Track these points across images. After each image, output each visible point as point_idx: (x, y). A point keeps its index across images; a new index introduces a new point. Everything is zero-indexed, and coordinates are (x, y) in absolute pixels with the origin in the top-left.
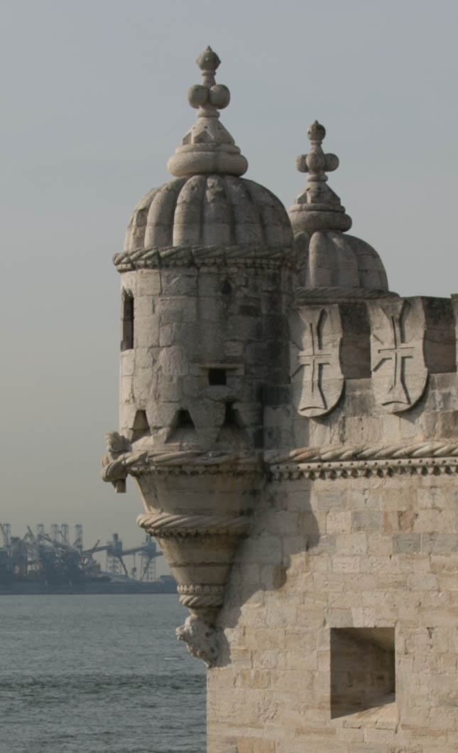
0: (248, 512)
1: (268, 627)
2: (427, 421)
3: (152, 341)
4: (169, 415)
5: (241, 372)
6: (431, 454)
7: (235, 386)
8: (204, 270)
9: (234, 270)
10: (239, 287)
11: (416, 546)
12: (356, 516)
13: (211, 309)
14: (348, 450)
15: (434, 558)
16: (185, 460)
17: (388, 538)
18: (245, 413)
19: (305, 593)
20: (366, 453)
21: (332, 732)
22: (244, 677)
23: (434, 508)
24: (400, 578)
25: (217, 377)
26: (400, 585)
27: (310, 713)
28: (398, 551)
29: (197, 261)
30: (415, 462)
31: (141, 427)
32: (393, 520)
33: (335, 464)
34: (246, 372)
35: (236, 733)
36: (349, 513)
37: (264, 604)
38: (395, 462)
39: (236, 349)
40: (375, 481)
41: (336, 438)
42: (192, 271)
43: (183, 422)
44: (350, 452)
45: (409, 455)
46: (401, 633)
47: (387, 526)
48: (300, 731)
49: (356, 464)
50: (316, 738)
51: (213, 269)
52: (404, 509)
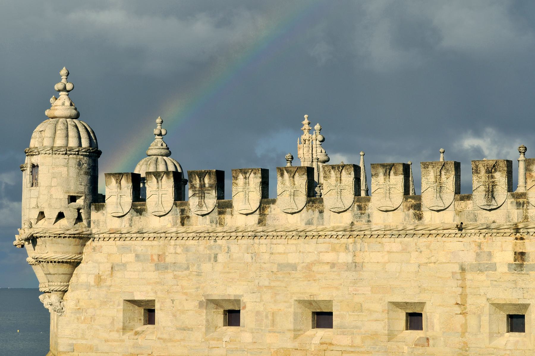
0: (81, 253)
1: (91, 299)
2: (173, 219)
5: (83, 198)
7: (80, 202)
8: (71, 156)
10: (83, 164)
11: (166, 268)
12: (137, 256)
14: (134, 230)
15: (175, 273)
17: (152, 264)
19: (110, 286)
20: (144, 231)
21: (123, 341)
22: (78, 319)
23: (176, 253)
24: (158, 280)
25: (73, 199)
27: (112, 333)
28: (158, 270)
29: (68, 152)
30: (167, 235)
32: (155, 258)
33: (127, 235)
34: (86, 198)
35: (74, 342)
36: (134, 254)
37: (89, 290)
38: (159, 235)
41: (127, 225)
43: (61, 216)
44: (137, 231)
46: (159, 301)
47: (152, 260)
48: (106, 341)
49: (138, 235)
50: (115, 343)
52: (161, 253)
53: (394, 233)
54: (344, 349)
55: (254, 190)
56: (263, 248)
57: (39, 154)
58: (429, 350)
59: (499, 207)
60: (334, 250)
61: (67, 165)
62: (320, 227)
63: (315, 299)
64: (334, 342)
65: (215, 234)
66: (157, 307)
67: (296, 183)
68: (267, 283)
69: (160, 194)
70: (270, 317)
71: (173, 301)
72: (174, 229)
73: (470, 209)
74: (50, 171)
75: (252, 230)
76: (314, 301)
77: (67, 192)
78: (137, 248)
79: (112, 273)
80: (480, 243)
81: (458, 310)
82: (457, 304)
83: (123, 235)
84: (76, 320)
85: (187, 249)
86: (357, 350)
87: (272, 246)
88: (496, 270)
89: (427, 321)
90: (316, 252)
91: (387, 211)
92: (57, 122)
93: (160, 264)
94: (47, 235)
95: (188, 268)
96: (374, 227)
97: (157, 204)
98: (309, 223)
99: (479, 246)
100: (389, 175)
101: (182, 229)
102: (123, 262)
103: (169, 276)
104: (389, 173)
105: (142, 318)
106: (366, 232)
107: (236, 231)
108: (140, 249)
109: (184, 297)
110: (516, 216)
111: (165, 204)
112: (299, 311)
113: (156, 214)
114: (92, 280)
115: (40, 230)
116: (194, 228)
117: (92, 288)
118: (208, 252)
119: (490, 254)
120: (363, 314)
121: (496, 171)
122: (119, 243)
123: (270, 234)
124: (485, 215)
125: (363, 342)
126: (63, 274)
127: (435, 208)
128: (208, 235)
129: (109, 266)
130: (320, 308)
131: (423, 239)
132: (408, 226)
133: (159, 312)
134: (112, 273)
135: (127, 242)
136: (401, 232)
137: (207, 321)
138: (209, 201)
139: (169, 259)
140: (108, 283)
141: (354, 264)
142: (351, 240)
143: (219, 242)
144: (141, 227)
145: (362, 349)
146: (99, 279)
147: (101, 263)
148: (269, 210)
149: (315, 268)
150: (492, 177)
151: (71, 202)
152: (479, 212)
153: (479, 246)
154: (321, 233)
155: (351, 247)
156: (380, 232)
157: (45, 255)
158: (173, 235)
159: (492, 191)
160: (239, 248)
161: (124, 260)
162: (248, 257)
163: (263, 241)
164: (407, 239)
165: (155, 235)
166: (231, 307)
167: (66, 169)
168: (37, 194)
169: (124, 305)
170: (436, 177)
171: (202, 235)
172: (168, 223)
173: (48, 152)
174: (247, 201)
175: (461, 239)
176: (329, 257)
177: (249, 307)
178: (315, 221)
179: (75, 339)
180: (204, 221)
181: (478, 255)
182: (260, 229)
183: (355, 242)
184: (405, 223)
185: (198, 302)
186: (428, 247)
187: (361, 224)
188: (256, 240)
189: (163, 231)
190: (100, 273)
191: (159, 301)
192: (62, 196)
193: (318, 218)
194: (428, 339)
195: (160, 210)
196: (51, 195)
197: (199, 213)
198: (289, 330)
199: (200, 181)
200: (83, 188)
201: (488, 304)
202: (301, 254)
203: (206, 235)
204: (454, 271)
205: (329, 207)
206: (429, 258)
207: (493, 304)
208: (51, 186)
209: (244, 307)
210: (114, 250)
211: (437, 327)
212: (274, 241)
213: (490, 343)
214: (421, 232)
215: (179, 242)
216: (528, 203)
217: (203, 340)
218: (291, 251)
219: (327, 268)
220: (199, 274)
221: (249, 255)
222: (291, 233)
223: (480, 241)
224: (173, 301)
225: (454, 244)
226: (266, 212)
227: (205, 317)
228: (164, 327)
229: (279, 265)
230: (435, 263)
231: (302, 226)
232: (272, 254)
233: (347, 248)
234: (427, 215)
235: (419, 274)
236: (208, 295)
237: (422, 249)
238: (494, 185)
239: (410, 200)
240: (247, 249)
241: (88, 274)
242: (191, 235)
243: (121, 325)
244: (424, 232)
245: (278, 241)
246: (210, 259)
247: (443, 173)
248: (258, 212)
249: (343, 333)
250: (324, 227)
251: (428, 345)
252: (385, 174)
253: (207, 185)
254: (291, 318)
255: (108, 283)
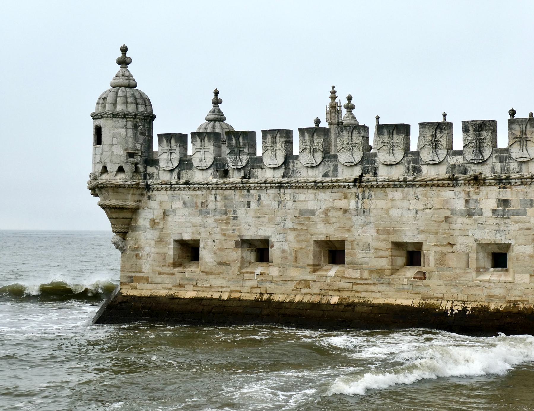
0: (140, 201)
3: (110, 142)
4: (116, 168)
5: (140, 154)
6: (217, 184)
7: (138, 159)
8: (128, 119)
9: (138, 120)
10: (139, 126)
11: (209, 213)
12: (184, 203)
13: (130, 133)
14: (182, 181)
15: (216, 217)
16: (122, 183)
18: (141, 167)
19: (163, 228)
21: (173, 274)
24: (202, 223)
25: (131, 155)
26: (201, 226)
27: (164, 268)
28: (201, 215)
31: (105, 170)
32: (199, 205)
35: (133, 274)
36: (182, 202)
37: (145, 232)
39: (139, 146)
40: (194, 192)
41: (177, 177)
42: (125, 120)
43: (121, 170)
45: (207, 184)
46: (202, 241)
47: (197, 207)
49: (185, 186)
51: (132, 119)
52: (203, 201)
53: (397, 183)
54: (354, 281)
55: (280, 148)
56: (288, 197)
57: (102, 117)
58: (425, 282)
59: (485, 161)
60: (346, 197)
61: (125, 127)
62: (335, 179)
63: (331, 239)
64: (346, 275)
65: (248, 185)
66: (201, 245)
67: (315, 142)
68: (291, 226)
69: (203, 151)
70: (294, 255)
71: (214, 241)
72: (215, 181)
73: (461, 163)
74: (111, 132)
75: (279, 181)
76: (330, 241)
77: (126, 149)
78: (184, 196)
79: (164, 218)
80: (469, 192)
81: (449, 249)
82: (449, 244)
83: (173, 186)
84: (135, 257)
85: (225, 198)
86: (366, 282)
87: (295, 194)
88: (482, 215)
89: (424, 259)
90: (331, 200)
91: (391, 165)
92: (119, 90)
93: (203, 209)
94: (109, 185)
95: (226, 213)
96: (380, 178)
97: (200, 161)
98: (325, 175)
99: (468, 194)
100: (393, 134)
101: (221, 181)
102: (173, 208)
103: (210, 220)
104: (393, 132)
105: (190, 255)
106: (373, 183)
107: (265, 182)
108: (187, 197)
109: (224, 238)
110: (500, 168)
111: (207, 161)
112: (318, 249)
113: (200, 168)
114: (147, 224)
115: (104, 181)
116: (231, 180)
117: (148, 230)
118: (243, 200)
119: (477, 201)
120: (371, 252)
121: (482, 130)
122: (170, 192)
123: (293, 184)
124: (473, 168)
125: (370, 275)
126: (123, 218)
127: (431, 162)
128: (243, 187)
129: (161, 212)
130: (336, 247)
131: (420, 189)
132: (408, 177)
133: (203, 249)
134: (164, 218)
135: (176, 192)
136: (402, 183)
137: (242, 257)
138: (243, 157)
139: (211, 206)
140: (161, 226)
141: (363, 210)
142: (360, 190)
143: (252, 192)
144: (187, 179)
145: (370, 282)
146: (154, 223)
147: (155, 209)
148: (292, 164)
149: (330, 214)
150: (480, 135)
151: (130, 157)
152: (468, 165)
153: (468, 194)
154: (335, 184)
155: (360, 196)
156: (384, 183)
157: (108, 202)
158: (213, 185)
159: (479, 148)
160: (269, 198)
161: (174, 206)
162: (275, 204)
163: (288, 191)
164: (406, 189)
165: (200, 186)
166: (261, 247)
167: (124, 130)
168: (100, 151)
169: (174, 244)
170: (432, 136)
171: (237, 185)
172: (209, 177)
173: (109, 116)
174: (274, 157)
175: (452, 189)
176: (342, 204)
177: (276, 245)
178: (331, 173)
179: (134, 272)
180: (239, 174)
181: (467, 201)
182: (285, 180)
183: (363, 192)
184: (406, 174)
185: (234, 242)
186: (425, 196)
187: (369, 177)
188: (282, 191)
189: (205, 182)
190: (154, 217)
191: (202, 241)
192: (122, 153)
193: (333, 171)
194: (424, 273)
195: (203, 164)
196: (113, 152)
197: (235, 167)
198: (309, 265)
199: (236, 140)
200: (140, 146)
201: (475, 244)
202: (319, 202)
203: (241, 185)
204: (446, 215)
205: (342, 162)
206: (425, 205)
207: (479, 244)
208: (113, 145)
209: (272, 246)
210: (166, 198)
211: (432, 263)
212: (297, 191)
213: (477, 277)
214: (418, 183)
215: (218, 192)
216: (510, 157)
217: (239, 273)
218: (310, 200)
219: (340, 213)
220: (235, 218)
221: (276, 203)
222: (310, 184)
223: (468, 190)
224: (214, 241)
225: (448, 193)
226: (290, 167)
227: (240, 254)
228: (206, 263)
229: (300, 211)
230: (430, 209)
231: (320, 179)
232: (295, 201)
233: (357, 196)
234: (424, 169)
235: (417, 218)
236: (242, 236)
237: (419, 197)
238: (481, 142)
239: (409, 155)
240: (275, 197)
241: (145, 219)
242: (228, 186)
243: (171, 261)
244: (421, 183)
245: (300, 190)
246: (244, 206)
247: (438, 132)
248: (283, 167)
249: (354, 268)
250: (338, 178)
251: (425, 278)
252: (389, 134)
253: (241, 144)
254: (311, 256)
255: (161, 226)
